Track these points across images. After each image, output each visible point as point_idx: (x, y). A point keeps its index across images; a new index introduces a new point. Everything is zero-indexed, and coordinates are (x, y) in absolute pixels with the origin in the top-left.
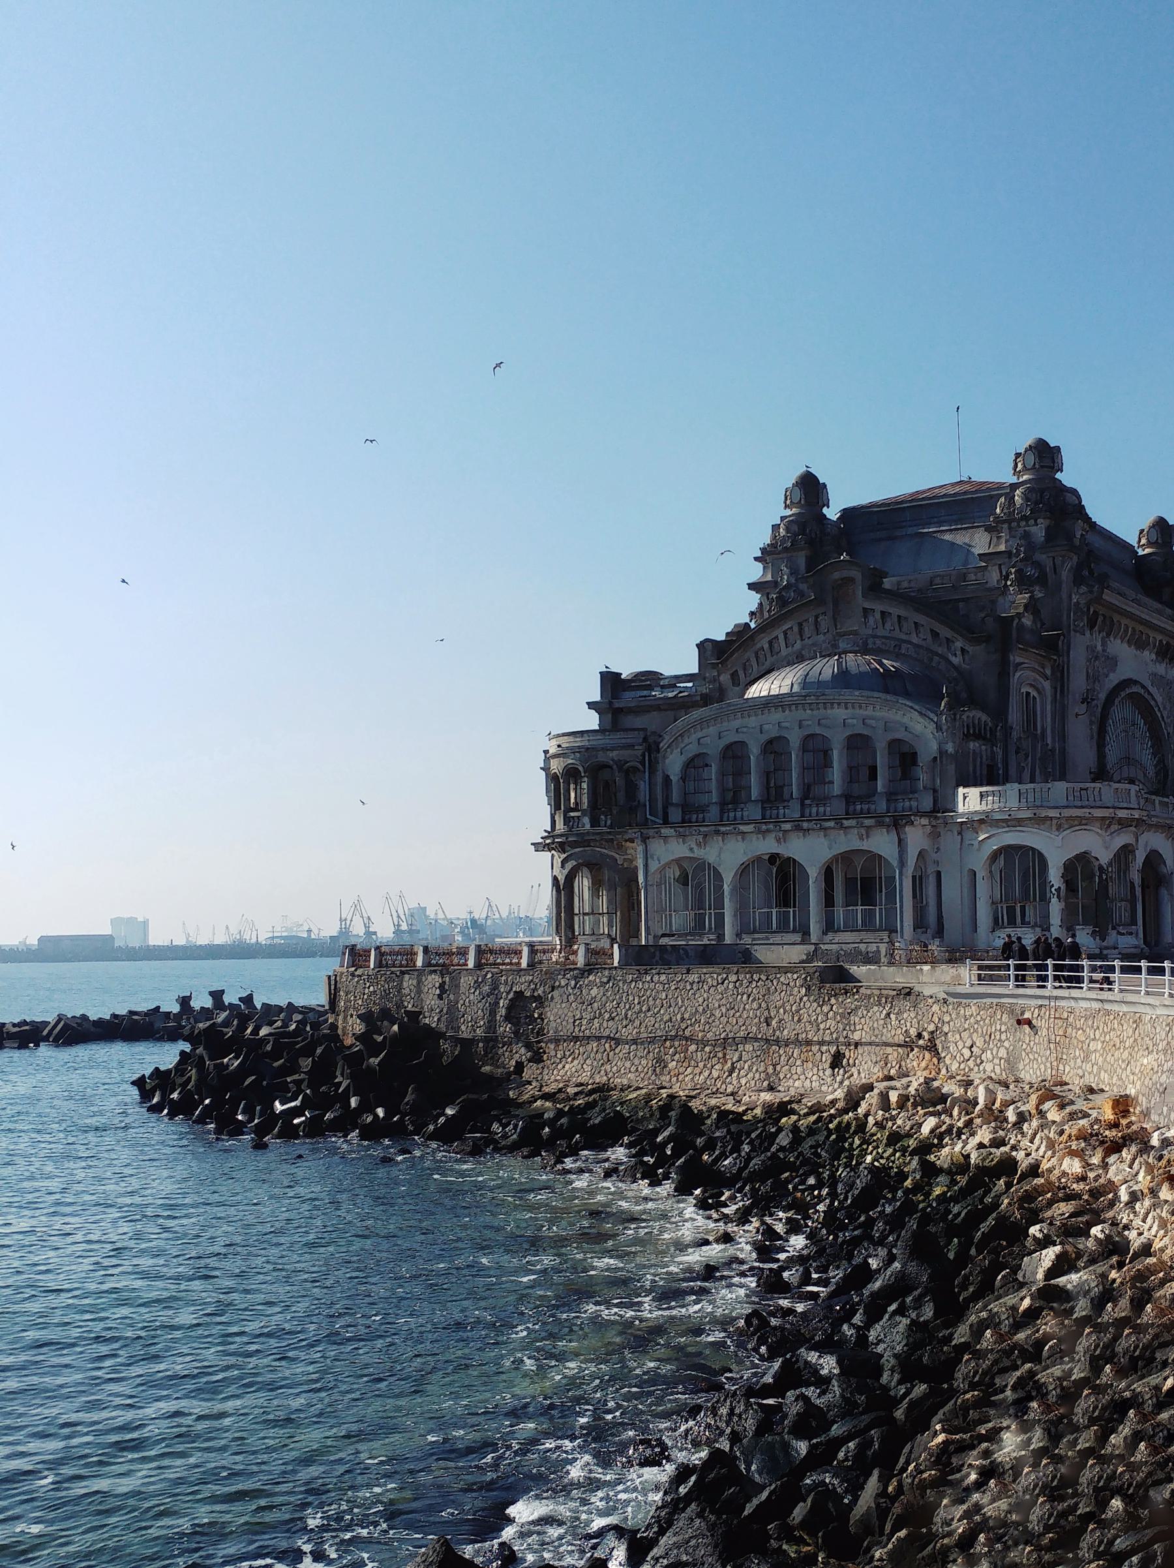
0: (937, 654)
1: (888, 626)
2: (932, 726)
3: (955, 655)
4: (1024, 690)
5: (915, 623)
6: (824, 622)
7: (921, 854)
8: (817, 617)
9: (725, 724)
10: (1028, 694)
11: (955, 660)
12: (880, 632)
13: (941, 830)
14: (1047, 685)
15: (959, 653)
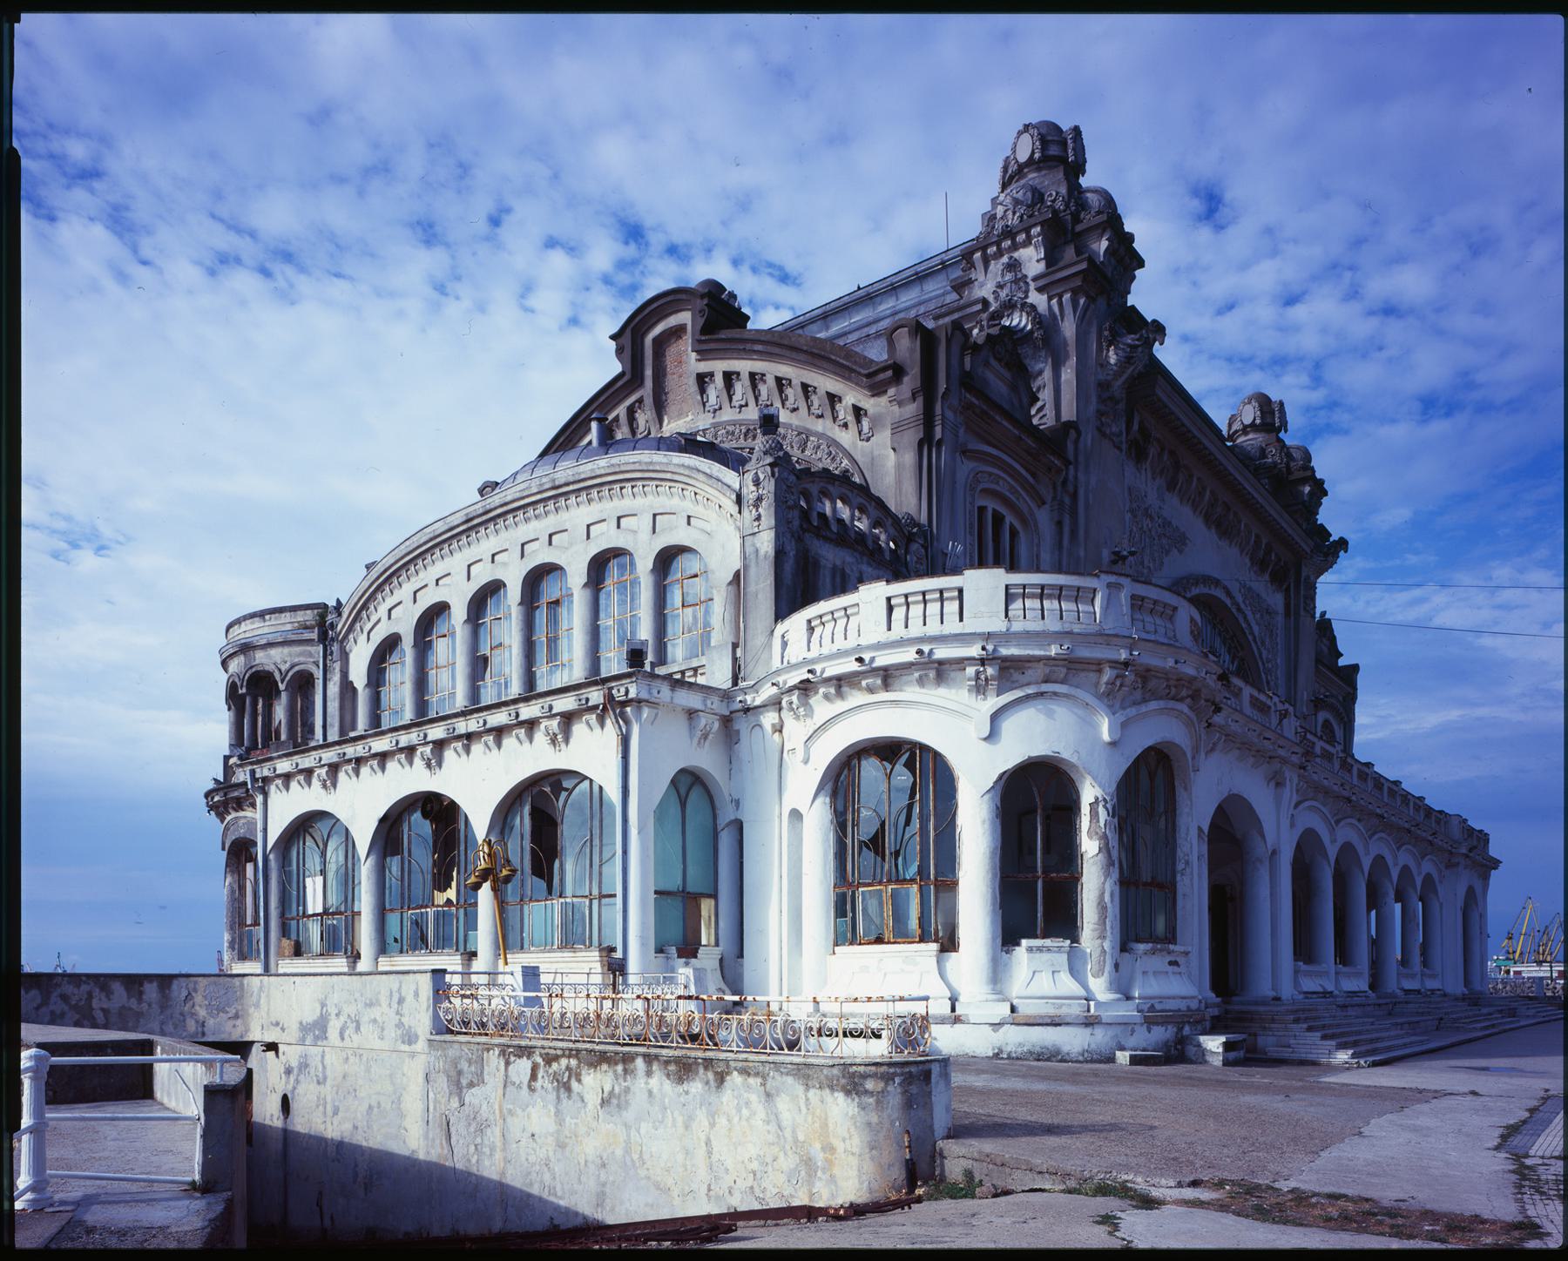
0: (817, 434)
1: (737, 397)
2: (730, 505)
3: (845, 425)
4: (991, 505)
5: (779, 380)
6: (642, 418)
7: (689, 783)
8: (631, 412)
9: (421, 574)
10: (998, 519)
11: (847, 438)
12: (727, 415)
13: (742, 725)
14: (1044, 517)
15: (850, 418)
